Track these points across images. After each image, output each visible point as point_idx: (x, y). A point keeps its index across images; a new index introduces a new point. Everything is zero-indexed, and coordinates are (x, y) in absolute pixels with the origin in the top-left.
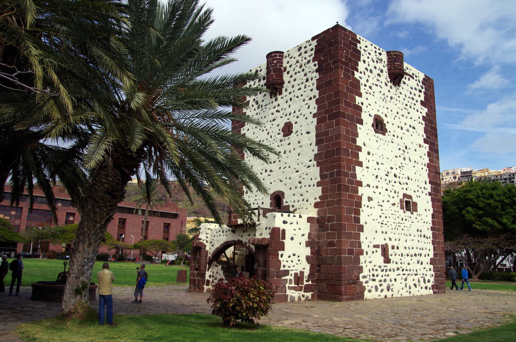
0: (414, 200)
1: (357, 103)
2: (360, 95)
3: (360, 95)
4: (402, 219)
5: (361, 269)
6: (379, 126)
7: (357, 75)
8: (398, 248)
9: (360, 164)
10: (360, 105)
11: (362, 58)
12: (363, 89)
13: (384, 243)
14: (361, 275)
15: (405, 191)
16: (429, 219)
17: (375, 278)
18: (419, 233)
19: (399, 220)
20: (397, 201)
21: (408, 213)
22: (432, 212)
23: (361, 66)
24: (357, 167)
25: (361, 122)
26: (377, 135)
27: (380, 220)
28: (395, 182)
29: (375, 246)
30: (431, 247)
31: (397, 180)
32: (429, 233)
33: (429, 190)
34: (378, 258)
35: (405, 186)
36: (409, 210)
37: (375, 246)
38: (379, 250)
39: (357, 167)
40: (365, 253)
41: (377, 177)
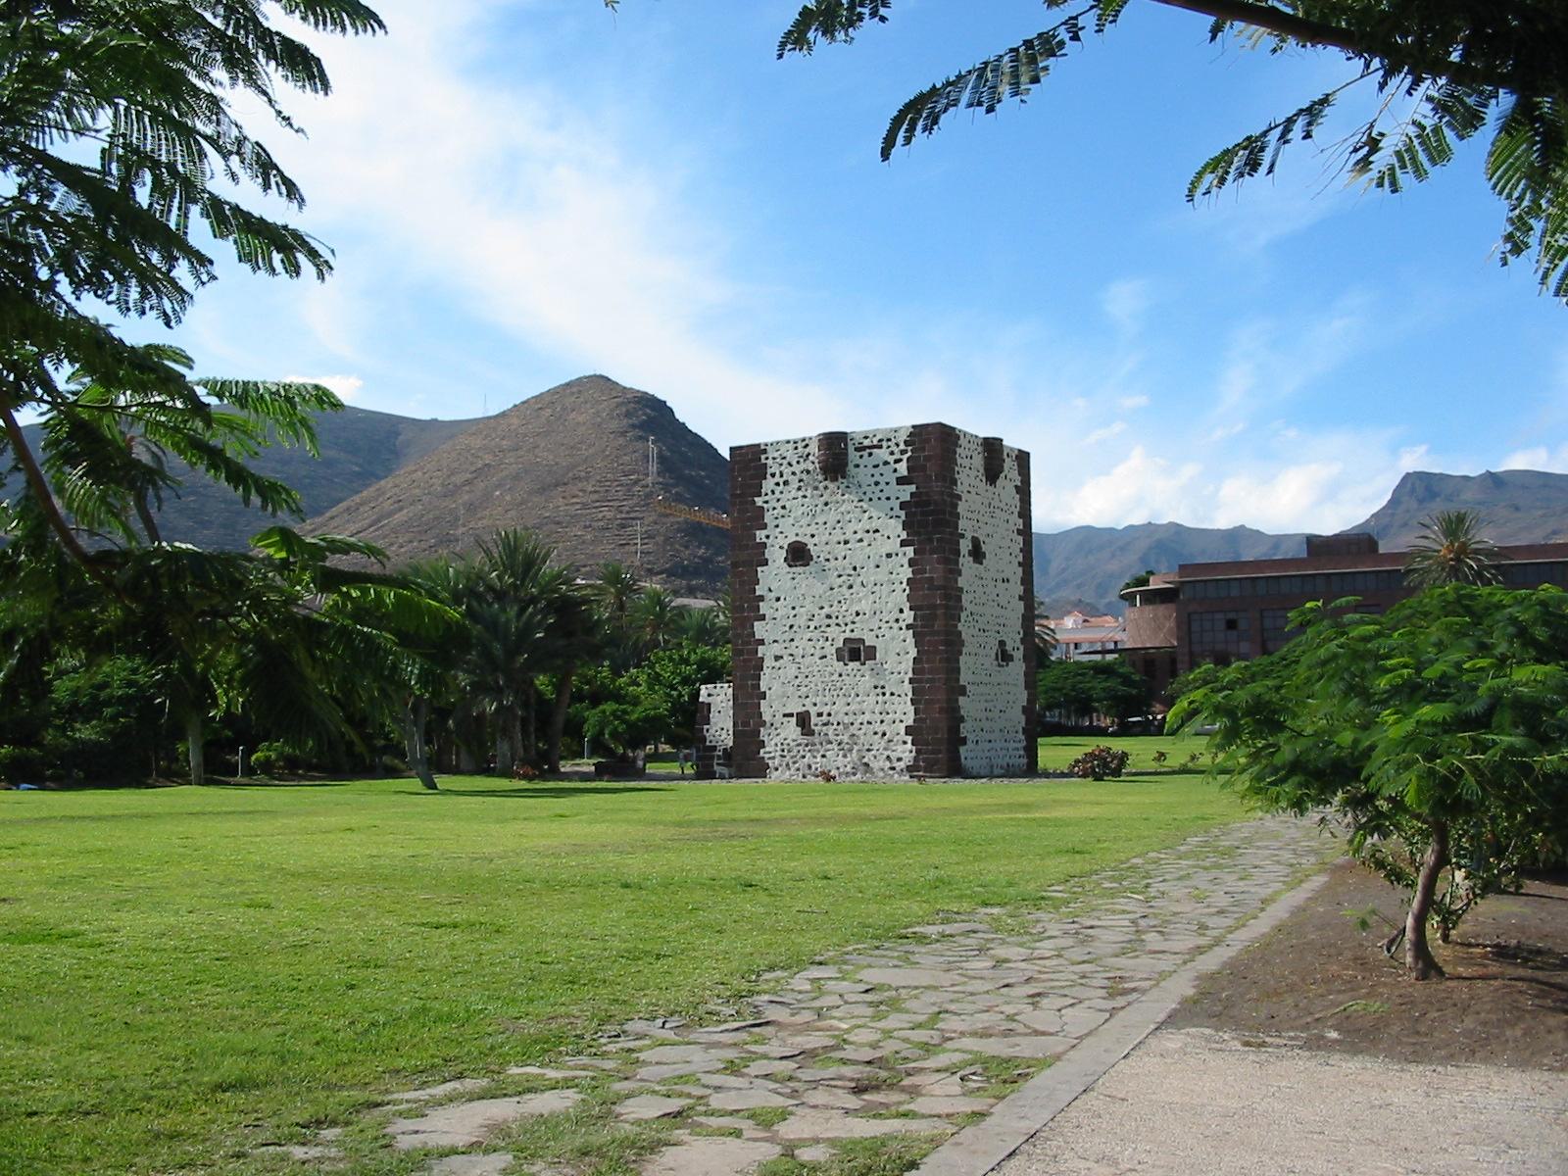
0: (867, 644)
1: (758, 540)
2: (765, 527)
3: (765, 527)
4: (840, 675)
5: (762, 744)
6: (798, 554)
7: (759, 501)
8: (829, 715)
9: (763, 618)
10: (764, 540)
11: (769, 471)
12: (768, 518)
13: (801, 709)
14: (762, 751)
15: (848, 635)
16: (907, 665)
17: (785, 753)
18: (879, 690)
19: (835, 677)
20: (831, 651)
21: (857, 664)
22: (913, 653)
23: (768, 484)
24: (756, 623)
25: (765, 563)
26: (794, 569)
27: (797, 682)
28: (829, 626)
29: (785, 715)
30: (911, 709)
31: (833, 621)
32: (907, 687)
33: (910, 621)
34: (792, 730)
35: (850, 627)
36: (859, 659)
37: (785, 715)
38: (794, 719)
39: (756, 623)
40: (768, 725)
41: (791, 627)
